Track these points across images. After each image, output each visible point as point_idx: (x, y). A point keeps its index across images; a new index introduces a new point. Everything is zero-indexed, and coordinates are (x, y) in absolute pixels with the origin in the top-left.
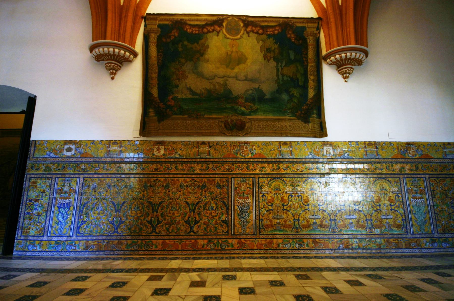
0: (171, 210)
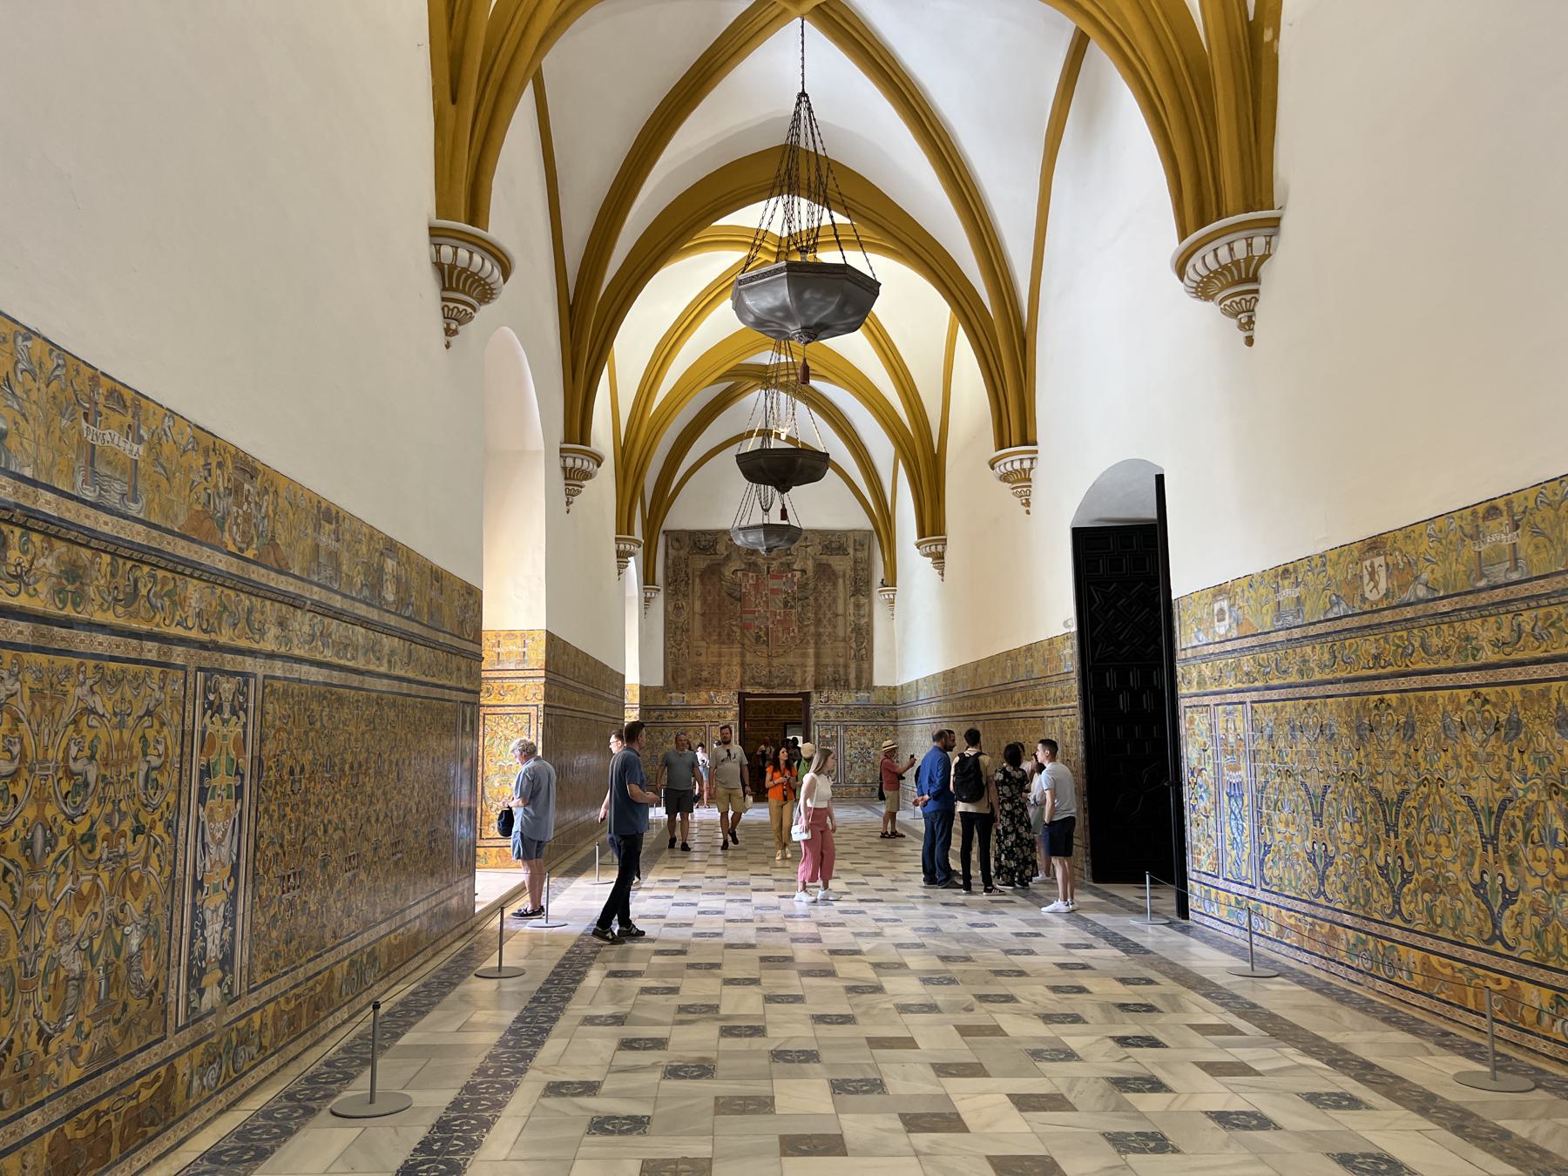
0: (1429, 830)
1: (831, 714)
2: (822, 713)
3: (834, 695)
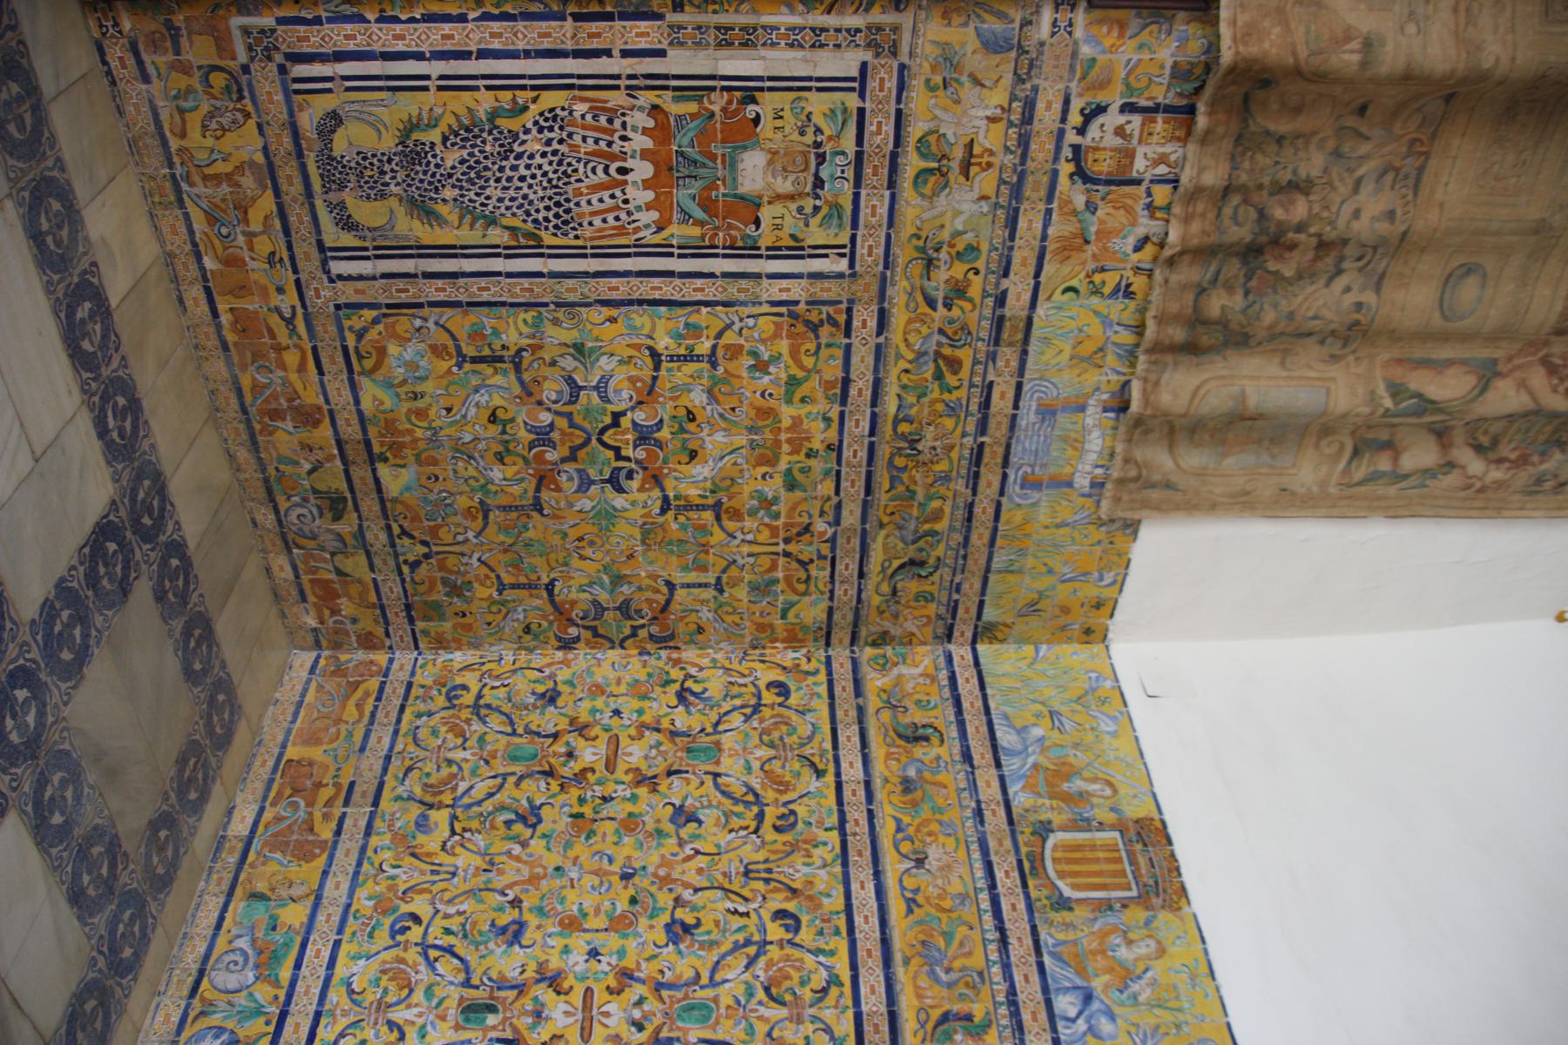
1: (964, 208)
2: (976, 116)
3: (1125, 228)
